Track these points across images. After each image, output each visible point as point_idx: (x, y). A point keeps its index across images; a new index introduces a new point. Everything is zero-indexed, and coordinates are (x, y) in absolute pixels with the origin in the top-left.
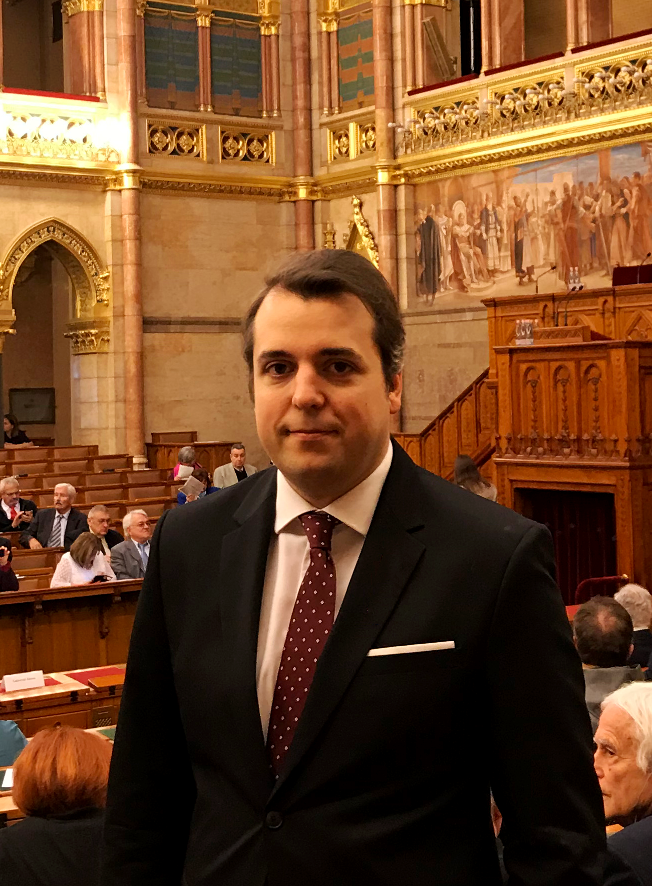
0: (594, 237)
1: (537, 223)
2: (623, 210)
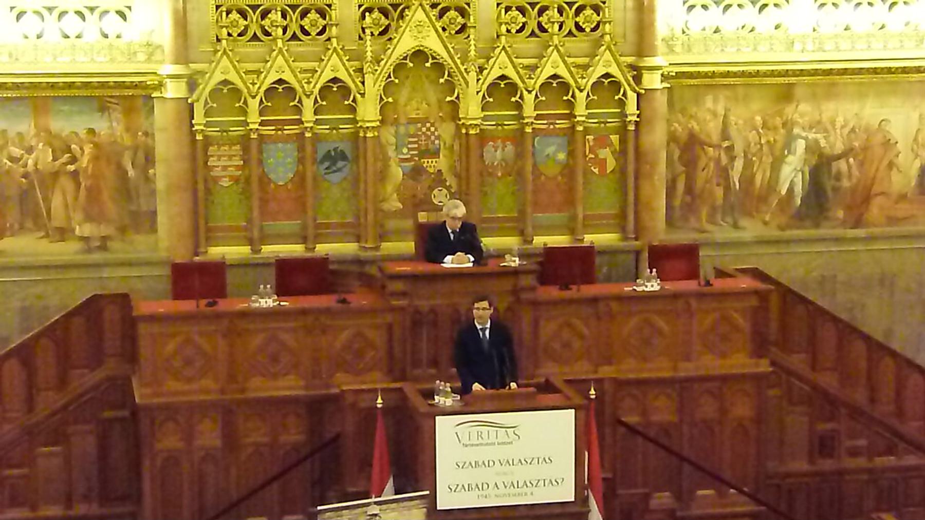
0: (25, 196)
2: (71, 168)
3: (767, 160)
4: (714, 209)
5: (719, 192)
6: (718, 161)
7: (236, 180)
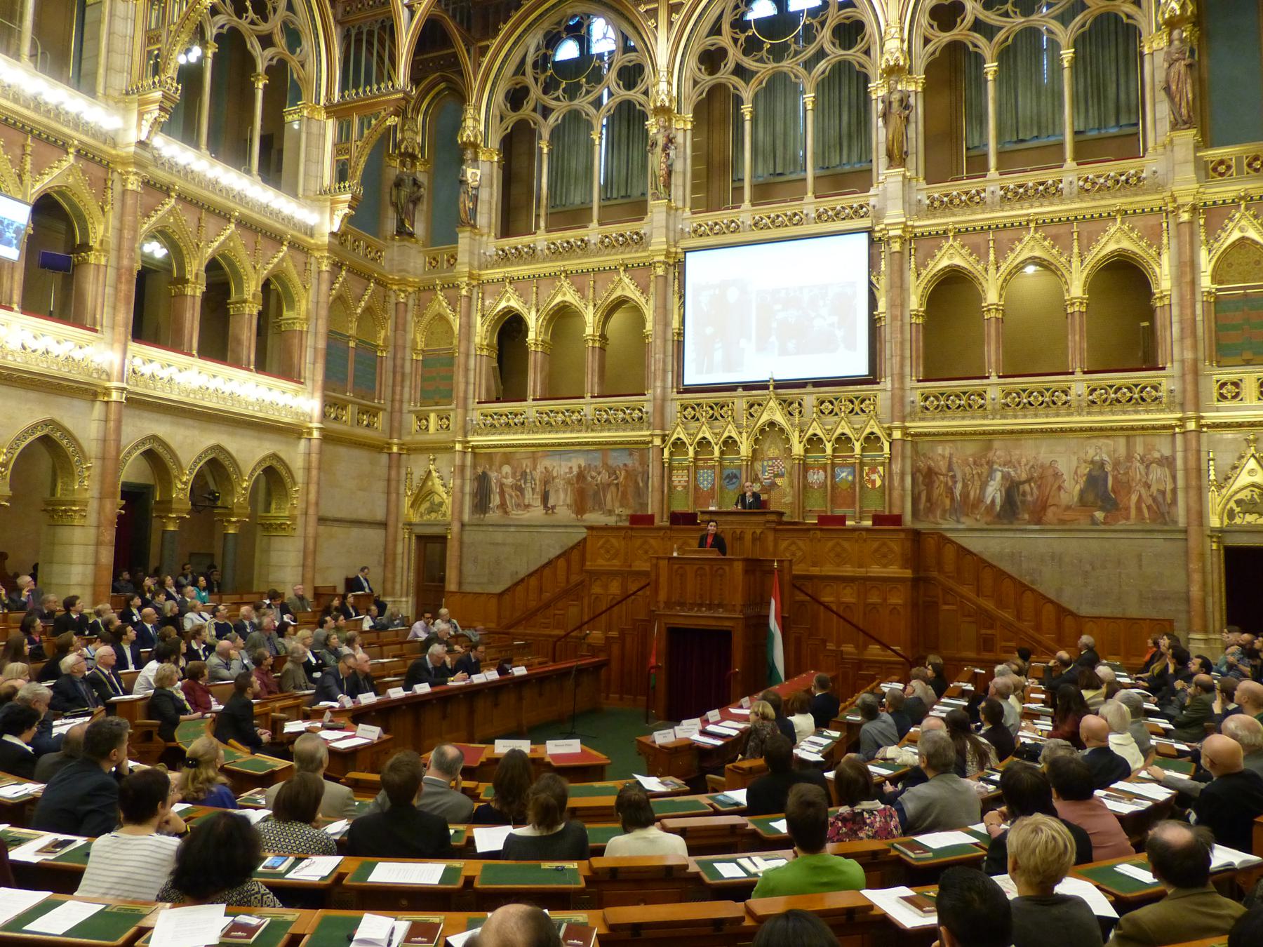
1: (560, 483)
3: (978, 484)
4: (944, 511)
5: (948, 502)
6: (946, 484)
7: (684, 487)
